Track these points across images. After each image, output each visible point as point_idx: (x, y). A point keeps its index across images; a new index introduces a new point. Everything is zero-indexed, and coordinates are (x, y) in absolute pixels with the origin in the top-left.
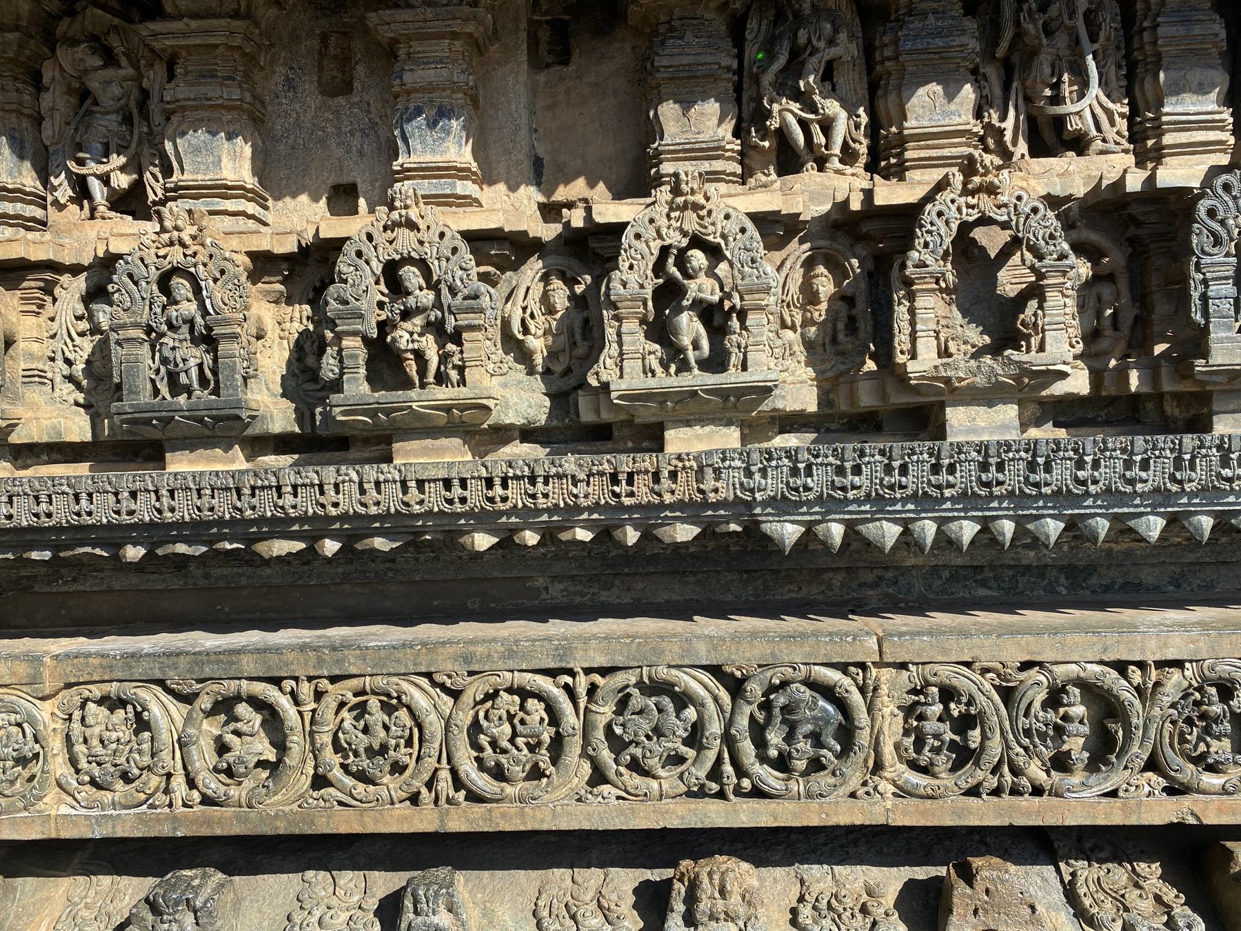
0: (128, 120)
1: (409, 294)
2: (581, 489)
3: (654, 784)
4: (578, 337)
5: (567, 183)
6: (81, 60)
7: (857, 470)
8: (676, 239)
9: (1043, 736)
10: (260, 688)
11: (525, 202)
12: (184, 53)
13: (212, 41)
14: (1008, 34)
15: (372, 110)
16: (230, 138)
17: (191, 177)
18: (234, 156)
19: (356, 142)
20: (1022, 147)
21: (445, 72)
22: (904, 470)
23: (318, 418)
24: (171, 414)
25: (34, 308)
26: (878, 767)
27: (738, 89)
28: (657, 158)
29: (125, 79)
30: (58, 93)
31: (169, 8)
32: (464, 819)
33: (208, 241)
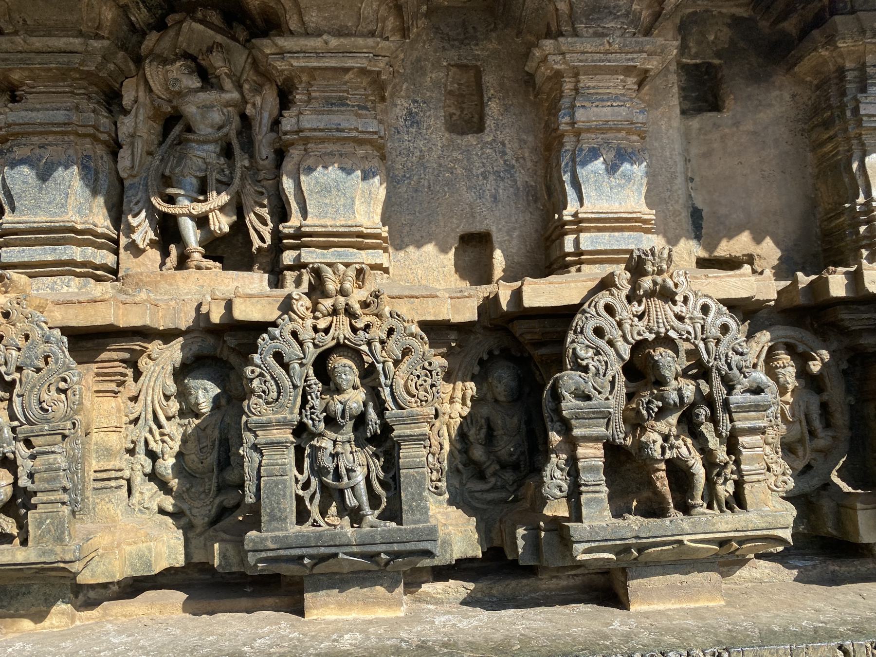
0: (227, 152)
1: (661, 382)
4: (817, 424)
5: (730, 238)
6: (176, 79)
11: (686, 256)
12: (305, 78)
13: (349, 63)
15: (508, 151)
16: (365, 178)
17: (317, 222)
18: (369, 197)
19: (490, 185)
21: (624, 112)
23: (521, 543)
24: (333, 550)
25: (113, 386)
29: (227, 104)
30: (141, 117)
31: (294, 25)
33: (387, 310)
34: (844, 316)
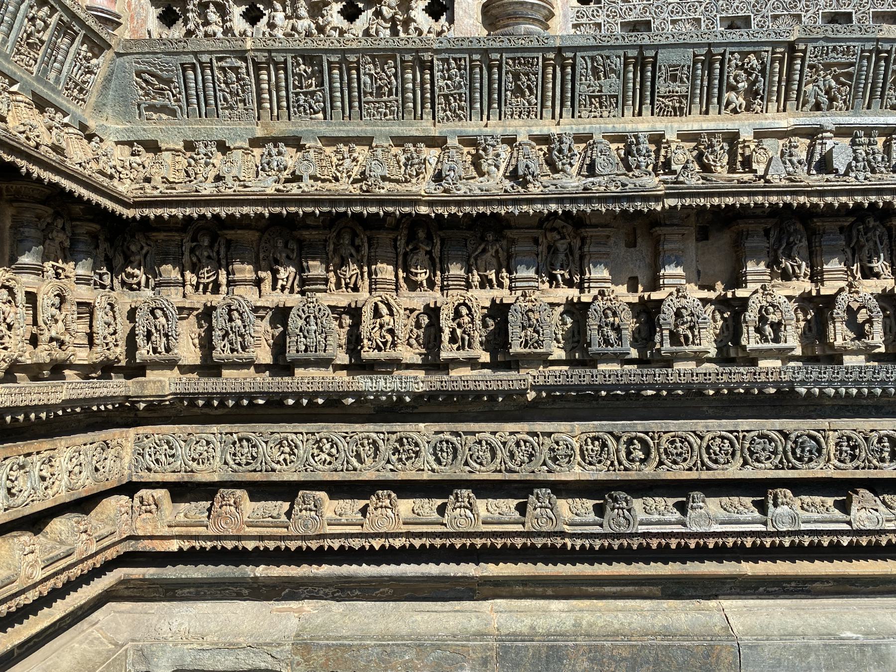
0: (566, 255)
2: (745, 377)
3: (763, 465)
7: (825, 373)
8: (764, 303)
9: (877, 451)
10: (642, 435)
14: (855, 241)
19: (638, 263)
20: (859, 275)
22: (838, 373)
26: (829, 460)
27: (768, 252)
28: (745, 274)
31: (588, 222)
32: (705, 475)
34: (732, 302)
